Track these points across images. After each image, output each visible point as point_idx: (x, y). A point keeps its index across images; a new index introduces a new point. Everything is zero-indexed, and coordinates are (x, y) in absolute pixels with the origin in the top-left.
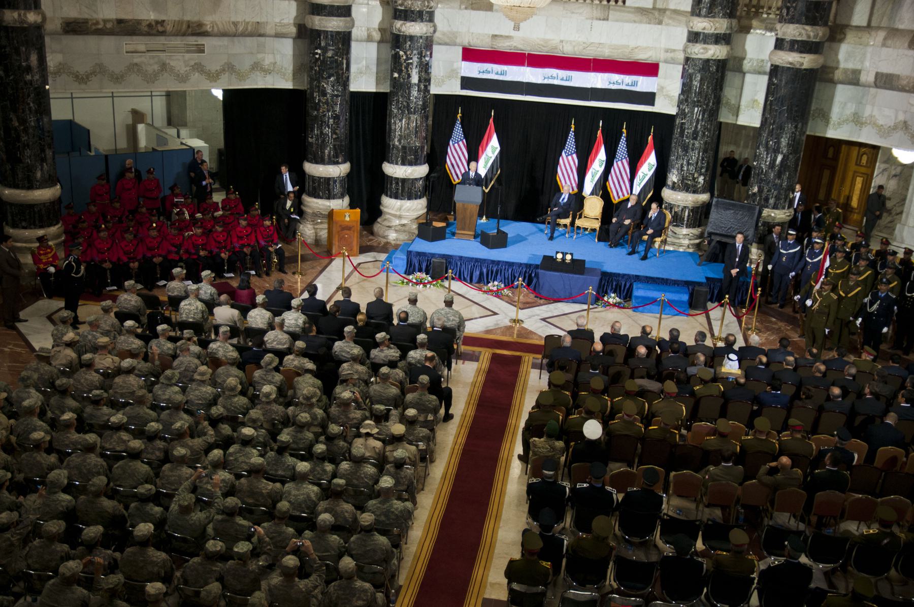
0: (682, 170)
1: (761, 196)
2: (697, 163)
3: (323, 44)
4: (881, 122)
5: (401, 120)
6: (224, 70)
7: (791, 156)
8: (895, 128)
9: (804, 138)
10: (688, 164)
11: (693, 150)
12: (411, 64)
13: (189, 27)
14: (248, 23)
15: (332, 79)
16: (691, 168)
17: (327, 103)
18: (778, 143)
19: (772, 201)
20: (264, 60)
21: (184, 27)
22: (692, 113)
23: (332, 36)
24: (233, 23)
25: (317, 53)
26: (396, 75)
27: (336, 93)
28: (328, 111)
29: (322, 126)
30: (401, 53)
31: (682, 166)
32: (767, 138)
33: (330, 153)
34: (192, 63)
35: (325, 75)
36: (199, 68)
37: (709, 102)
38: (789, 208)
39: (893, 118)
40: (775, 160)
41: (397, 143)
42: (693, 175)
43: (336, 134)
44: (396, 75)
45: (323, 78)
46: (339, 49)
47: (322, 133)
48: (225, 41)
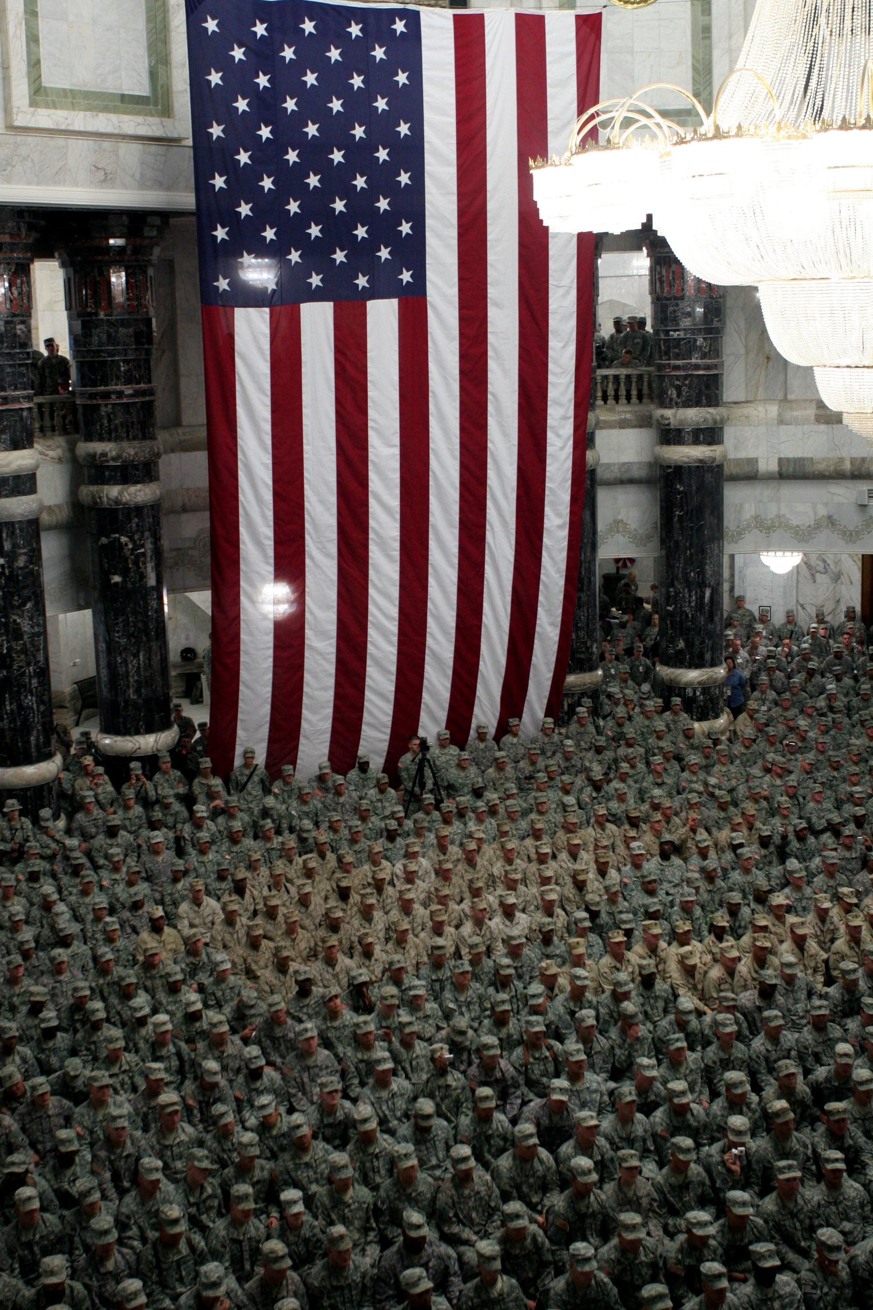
3: (7, 546)
4: (795, 522)
5: (136, 655)
8: (817, 526)
12: (144, 554)
15: (29, 605)
19: (708, 656)
23: (21, 530)
28: (29, 664)
29: (19, 693)
30: (124, 539)
32: (684, 569)
33: (37, 739)
39: (811, 514)
40: (702, 597)
41: (133, 697)
42: (585, 643)
45: (13, 607)
47: (20, 706)
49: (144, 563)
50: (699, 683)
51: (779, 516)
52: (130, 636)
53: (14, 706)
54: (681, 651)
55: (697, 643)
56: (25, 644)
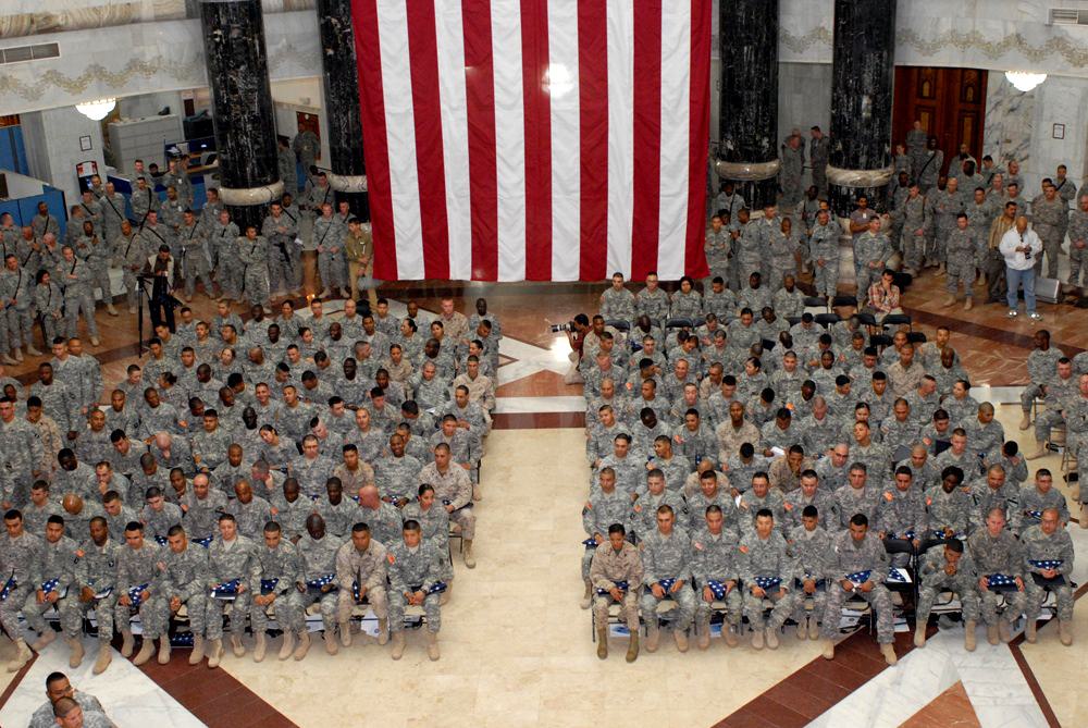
0: (739, 133)
1: (847, 155)
2: (757, 121)
3: (223, 21)
4: (987, 39)
5: (345, 113)
6: (89, 76)
7: (879, 96)
8: (1007, 44)
9: (893, 72)
10: (746, 123)
11: (749, 103)
12: (350, 33)
13: (32, 22)
14: (114, 7)
15: (242, 68)
16: (750, 128)
17: (239, 102)
18: (860, 81)
19: (863, 160)
20: (143, 54)
21: (26, 23)
22: (742, 55)
23: (234, 9)
24: (94, 9)
25: (216, 36)
26: (331, 52)
27: (250, 87)
28: (243, 113)
29: (237, 134)
30: (334, 21)
31: (737, 128)
32: (845, 75)
33: (253, 170)
34: (44, 71)
35: (232, 64)
36: (54, 77)
37: (761, 37)
38: (886, 166)
39: (1002, 31)
40: (859, 104)
41: (344, 146)
43: (257, 143)
44: (331, 52)
45: (230, 68)
46: (246, 25)
47: (238, 144)
48: (85, 36)
49: (351, 41)
50: (851, 183)
51: (973, 32)
52: (341, 98)
53: (233, 144)
54: (839, 152)
55: (853, 146)
56: (240, 97)
